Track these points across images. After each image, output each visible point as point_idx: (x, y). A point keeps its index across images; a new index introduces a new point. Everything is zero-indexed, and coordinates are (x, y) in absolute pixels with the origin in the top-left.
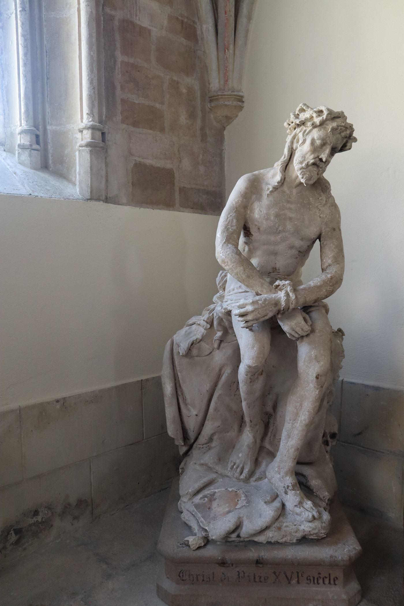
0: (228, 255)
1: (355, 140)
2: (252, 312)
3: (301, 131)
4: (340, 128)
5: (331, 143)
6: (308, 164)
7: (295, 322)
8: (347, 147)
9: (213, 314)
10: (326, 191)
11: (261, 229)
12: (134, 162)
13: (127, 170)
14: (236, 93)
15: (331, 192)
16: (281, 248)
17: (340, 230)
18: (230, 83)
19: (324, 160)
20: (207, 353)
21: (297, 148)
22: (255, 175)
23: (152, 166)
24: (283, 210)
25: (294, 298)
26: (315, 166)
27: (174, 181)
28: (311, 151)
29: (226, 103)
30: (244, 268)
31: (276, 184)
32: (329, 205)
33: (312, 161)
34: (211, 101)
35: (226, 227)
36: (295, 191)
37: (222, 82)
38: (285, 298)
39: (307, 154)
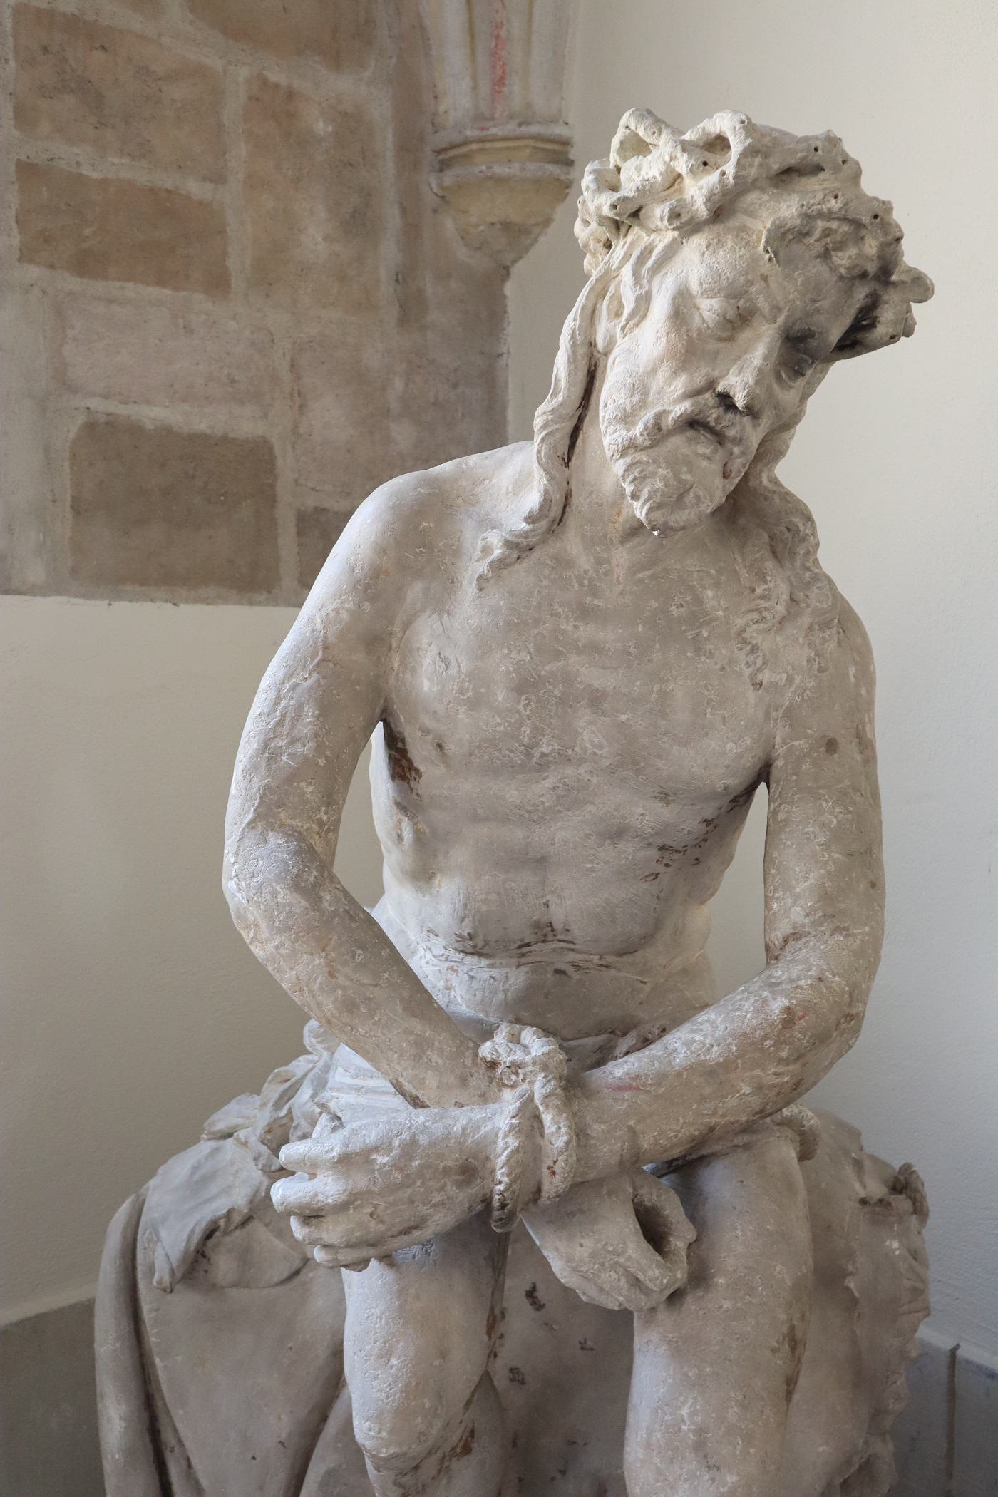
0: (259, 889)
1: (921, 288)
2: (341, 1208)
3: (627, 256)
4: (820, 224)
5: (777, 309)
6: (657, 426)
7: (589, 1244)
8: (881, 330)
9: (290, 1111)
10: (792, 554)
11: (451, 748)
12: (82, 419)
13: (46, 449)
14: (534, 129)
15: (820, 555)
16: (562, 833)
17: (865, 745)
18: (515, 87)
19: (740, 402)
20: (283, 1271)
21: (611, 343)
22: (434, 483)
23: (167, 433)
24: (558, 655)
25: (560, 1142)
26: (703, 436)
27: (272, 487)
28: (671, 354)
29: (498, 170)
30: (330, 963)
31: (524, 526)
32: (806, 620)
33: (681, 409)
34: (444, 166)
35: (265, 746)
36: (622, 558)
37: (485, 89)
38: (513, 1143)
39: (654, 370)
